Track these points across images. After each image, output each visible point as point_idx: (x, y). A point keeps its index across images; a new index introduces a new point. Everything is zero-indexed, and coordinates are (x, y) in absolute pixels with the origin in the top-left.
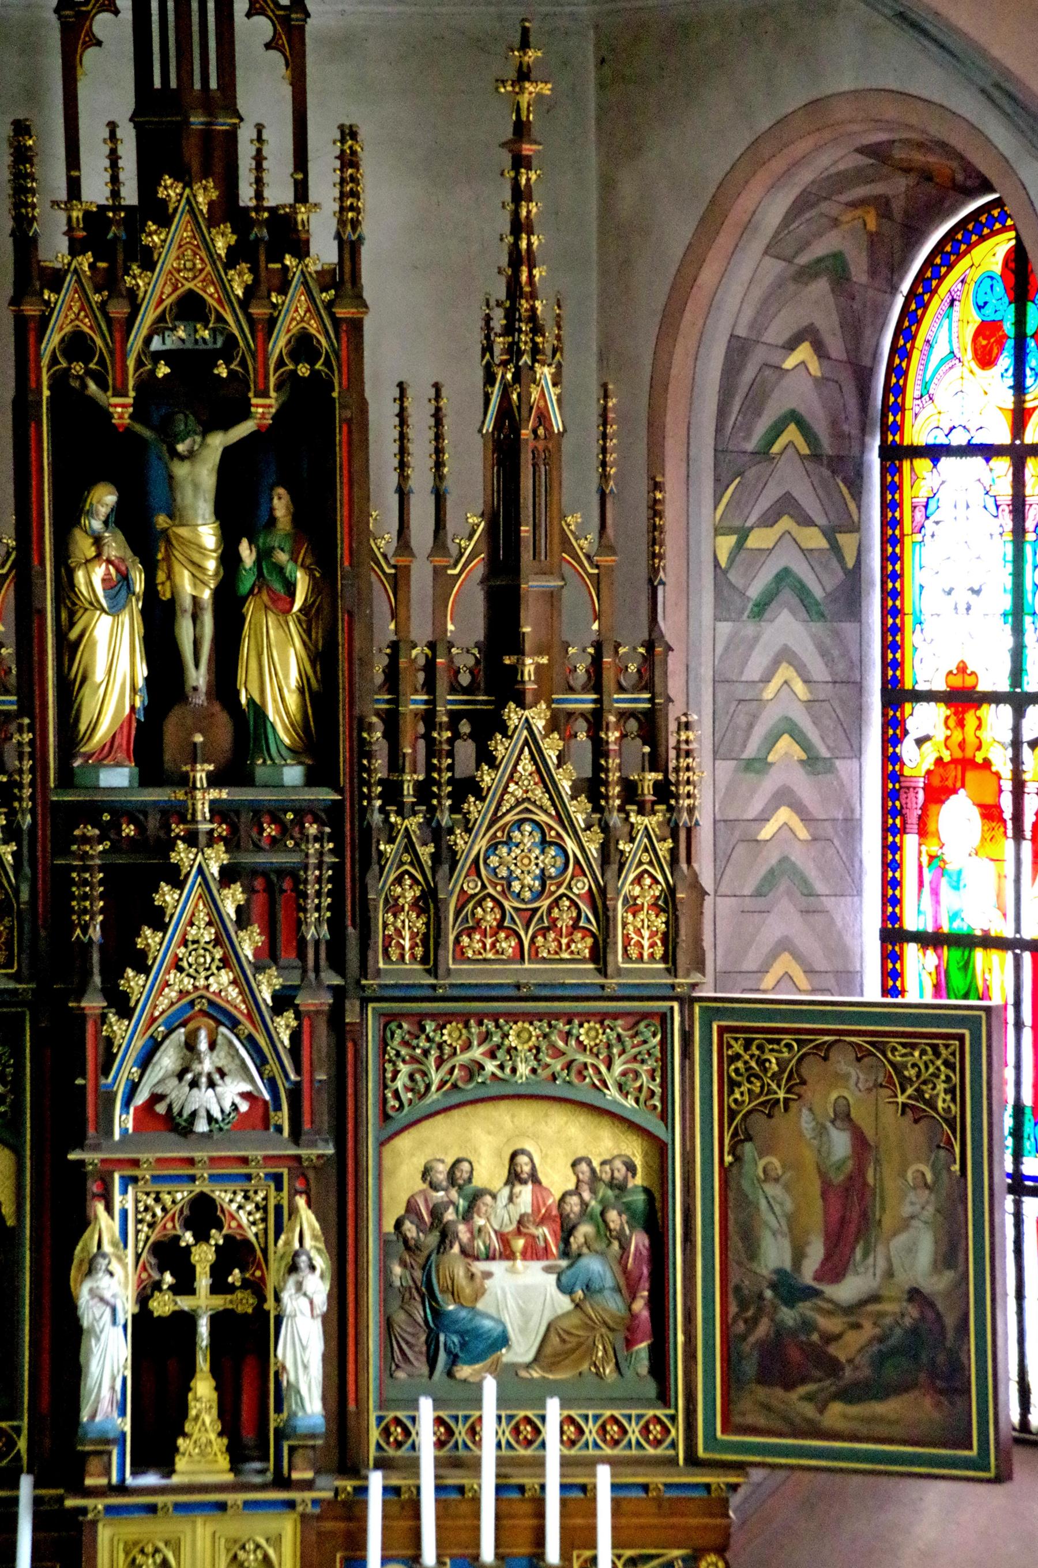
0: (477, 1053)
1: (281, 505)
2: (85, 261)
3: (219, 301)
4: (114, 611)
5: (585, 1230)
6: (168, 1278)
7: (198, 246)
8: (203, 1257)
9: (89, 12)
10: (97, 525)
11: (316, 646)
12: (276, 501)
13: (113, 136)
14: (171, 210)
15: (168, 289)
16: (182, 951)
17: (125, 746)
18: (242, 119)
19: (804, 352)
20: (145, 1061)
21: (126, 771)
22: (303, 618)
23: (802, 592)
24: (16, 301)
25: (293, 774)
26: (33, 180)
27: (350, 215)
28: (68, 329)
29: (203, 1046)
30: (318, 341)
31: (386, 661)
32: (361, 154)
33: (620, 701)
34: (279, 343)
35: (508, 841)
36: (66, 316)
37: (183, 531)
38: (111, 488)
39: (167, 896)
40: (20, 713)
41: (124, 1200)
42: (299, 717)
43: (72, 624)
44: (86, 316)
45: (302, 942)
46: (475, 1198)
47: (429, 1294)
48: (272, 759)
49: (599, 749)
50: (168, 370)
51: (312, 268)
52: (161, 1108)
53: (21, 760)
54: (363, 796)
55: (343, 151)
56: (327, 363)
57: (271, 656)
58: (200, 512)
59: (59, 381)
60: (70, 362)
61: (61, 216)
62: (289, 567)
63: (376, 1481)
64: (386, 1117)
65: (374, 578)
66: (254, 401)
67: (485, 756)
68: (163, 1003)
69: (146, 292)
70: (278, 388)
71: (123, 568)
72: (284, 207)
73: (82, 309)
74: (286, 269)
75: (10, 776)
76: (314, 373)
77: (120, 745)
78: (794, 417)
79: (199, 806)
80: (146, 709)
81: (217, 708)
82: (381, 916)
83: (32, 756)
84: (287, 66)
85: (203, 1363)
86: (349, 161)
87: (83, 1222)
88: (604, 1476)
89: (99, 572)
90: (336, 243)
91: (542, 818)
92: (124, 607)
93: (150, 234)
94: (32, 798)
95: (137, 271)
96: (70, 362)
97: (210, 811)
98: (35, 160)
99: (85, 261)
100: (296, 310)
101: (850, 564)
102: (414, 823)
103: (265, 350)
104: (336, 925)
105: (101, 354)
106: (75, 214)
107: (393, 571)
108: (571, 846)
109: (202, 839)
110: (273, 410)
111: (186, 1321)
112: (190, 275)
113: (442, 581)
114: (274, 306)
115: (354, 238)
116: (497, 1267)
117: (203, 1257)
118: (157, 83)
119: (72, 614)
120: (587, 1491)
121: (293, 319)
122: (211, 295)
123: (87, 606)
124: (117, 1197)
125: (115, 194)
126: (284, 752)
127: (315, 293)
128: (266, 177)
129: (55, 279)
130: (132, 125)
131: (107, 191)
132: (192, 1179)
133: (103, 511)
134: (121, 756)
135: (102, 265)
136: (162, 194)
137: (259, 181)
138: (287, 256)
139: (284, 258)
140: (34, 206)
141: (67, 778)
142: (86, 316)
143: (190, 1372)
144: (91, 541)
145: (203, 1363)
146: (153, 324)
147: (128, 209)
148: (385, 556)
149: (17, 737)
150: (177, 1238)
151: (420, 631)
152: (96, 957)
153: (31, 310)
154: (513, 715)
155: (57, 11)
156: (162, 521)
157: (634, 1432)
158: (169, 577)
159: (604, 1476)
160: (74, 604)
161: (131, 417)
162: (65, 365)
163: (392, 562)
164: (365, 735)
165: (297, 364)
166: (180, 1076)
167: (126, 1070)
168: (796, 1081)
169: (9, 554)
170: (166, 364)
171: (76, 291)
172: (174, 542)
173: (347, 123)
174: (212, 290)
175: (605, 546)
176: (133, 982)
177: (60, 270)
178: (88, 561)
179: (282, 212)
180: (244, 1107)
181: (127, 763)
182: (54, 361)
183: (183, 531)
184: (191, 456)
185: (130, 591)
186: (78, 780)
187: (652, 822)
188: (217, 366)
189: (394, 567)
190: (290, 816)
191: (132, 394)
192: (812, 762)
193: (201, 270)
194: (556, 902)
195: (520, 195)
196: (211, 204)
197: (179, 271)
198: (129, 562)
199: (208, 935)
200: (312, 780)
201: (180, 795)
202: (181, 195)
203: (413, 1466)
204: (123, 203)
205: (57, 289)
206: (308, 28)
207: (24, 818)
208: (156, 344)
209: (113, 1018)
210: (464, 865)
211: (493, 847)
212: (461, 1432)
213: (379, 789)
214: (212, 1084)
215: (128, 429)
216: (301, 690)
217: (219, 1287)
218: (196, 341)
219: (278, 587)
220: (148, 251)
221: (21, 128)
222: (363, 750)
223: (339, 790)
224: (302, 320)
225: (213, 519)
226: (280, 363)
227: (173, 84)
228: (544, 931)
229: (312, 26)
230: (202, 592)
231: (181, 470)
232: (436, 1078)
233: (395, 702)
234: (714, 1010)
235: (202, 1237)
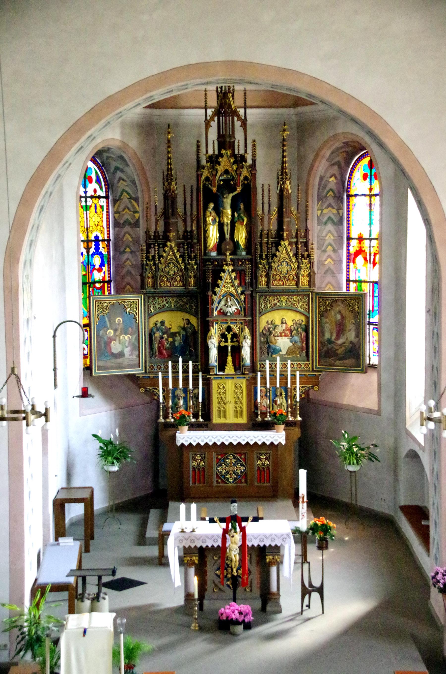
0: (276, 301)
1: (242, 206)
2: (209, 164)
4: (213, 225)
5: (294, 332)
6: (223, 340)
8: (229, 336)
10: (210, 210)
13: (214, 143)
16: (225, 284)
19: (333, 178)
20: (219, 303)
23: (333, 221)
24: (197, 171)
25: (244, 253)
29: (229, 300)
33: (301, 240)
34: (242, 178)
35: (281, 265)
37: (225, 211)
39: (222, 274)
40: (197, 243)
41: (216, 326)
45: (246, 282)
46: (275, 326)
47: (267, 343)
49: (297, 248)
52: (222, 311)
56: (250, 181)
59: (204, 185)
61: (205, 156)
63: (259, 374)
64: (260, 313)
67: (277, 250)
68: (222, 293)
70: (242, 185)
74: (243, 165)
76: (248, 183)
78: (331, 190)
82: (259, 278)
85: (229, 354)
86: (254, 146)
87: (209, 330)
88: (298, 373)
89: (211, 218)
91: (287, 260)
99: (209, 164)
101: (341, 215)
102: (265, 262)
104: (251, 279)
108: (292, 265)
109: (228, 265)
111: (226, 347)
113: (270, 219)
116: (279, 338)
117: (229, 336)
118: (221, 133)
119: (206, 226)
120: (295, 376)
124: (215, 326)
125: (214, 152)
129: (203, 167)
131: (212, 152)
132: (227, 323)
133: (211, 207)
136: (222, 152)
137: (239, 150)
141: (205, 254)
143: (227, 355)
145: (229, 354)
147: (216, 155)
150: (225, 333)
151: (266, 228)
152: (210, 285)
153: (199, 173)
154: (282, 243)
155: (205, 121)
156: (221, 209)
157: (303, 366)
158: (223, 219)
159: (298, 373)
166: (225, 305)
167: (216, 304)
168: (331, 306)
175: (298, 213)
176: (217, 289)
180: (236, 311)
182: (203, 182)
184: (226, 198)
185: (216, 221)
187: (306, 261)
192: (334, 251)
194: (289, 275)
195: (284, 151)
199: (229, 281)
200: (247, 254)
203: (265, 371)
205: (204, 169)
208: (221, 178)
209: (213, 295)
210: (274, 269)
211: (279, 266)
212: (273, 365)
214: (230, 307)
215: (216, 193)
217: (232, 341)
219: (241, 220)
221: (198, 142)
222: (256, 249)
226: (242, 181)
227: (224, 133)
228: (288, 280)
231: (225, 200)
232: (269, 306)
233: (261, 240)
234: (317, 294)
235: (229, 333)
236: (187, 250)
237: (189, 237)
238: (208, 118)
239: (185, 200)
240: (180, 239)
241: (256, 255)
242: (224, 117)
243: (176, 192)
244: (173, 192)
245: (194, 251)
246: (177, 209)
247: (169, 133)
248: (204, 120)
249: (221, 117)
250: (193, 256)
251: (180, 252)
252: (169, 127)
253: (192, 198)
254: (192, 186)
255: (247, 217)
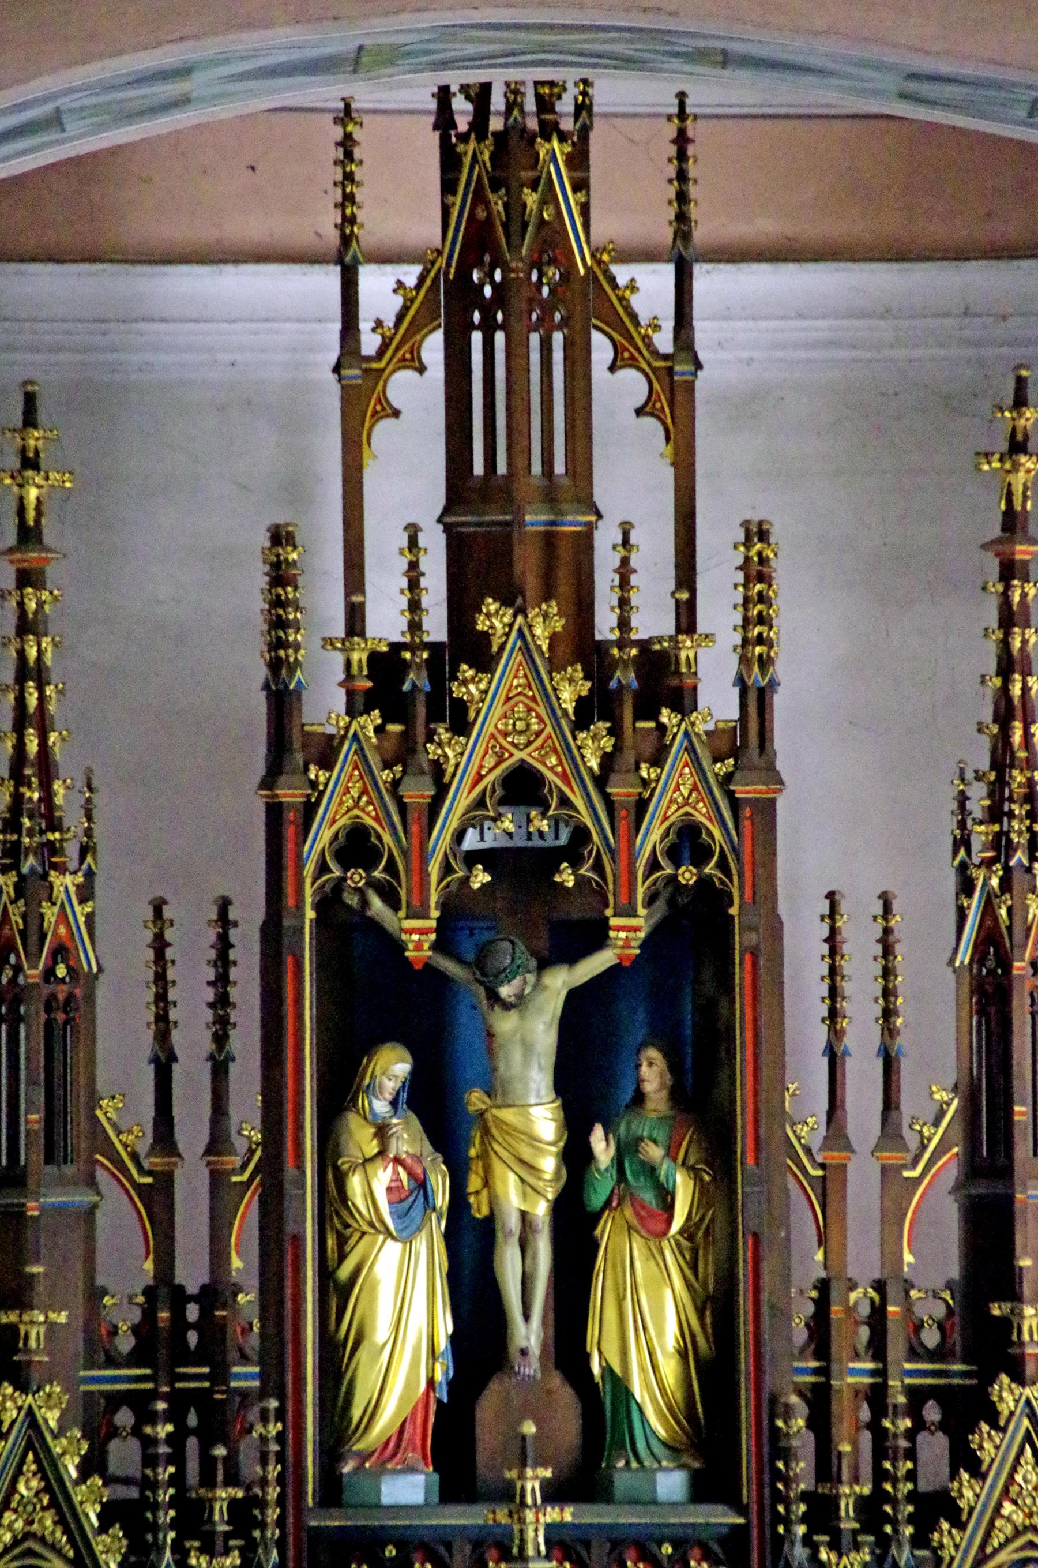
3: (564, 776)
4: (406, 1236)
7: (533, 699)
9: (383, 370)
10: (381, 1107)
11: (704, 1286)
12: (644, 1069)
13: (413, 544)
14: (495, 648)
15: (490, 761)
17: (418, 1443)
18: (600, 516)
21: (420, 1478)
22: (685, 1243)
24: (269, 782)
26: (297, 608)
27: (758, 650)
28: (342, 822)
30: (711, 835)
31: (810, 1309)
32: (773, 564)
36: (341, 803)
37: (507, 1115)
38: (402, 1052)
40: (263, 1394)
42: (679, 1396)
43: (342, 1257)
44: (370, 802)
48: (639, 1460)
50: (488, 878)
51: (701, 728)
53: (264, 1463)
54: (777, 1519)
55: (747, 559)
56: (723, 865)
57: (637, 1302)
58: (533, 1086)
60: (346, 869)
61: (339, 658)
62: (665, 1168)
65: (792, 1184)
66: (614, 922)
69: (457, 765)
70: (650, 900)
71: (419, 1171)
72: (660, 640)
73: (364, 792)
74: (662, 728)
75: (248, 1488)
76: (704, 882)
77: (412, 1441)
79: (531, 1534)
80: (451, 1384)
81: (556, 1380)
83: (280, 1458)
84: (668, 439)
89: (382, 1177)
90: (736, 691)
92: (419, 1229)
93: (465, 683)
94: (280, 1522)
95: (445, 736)
96: (346, 869)
97: (547, 1542)
98: (301, 581)
100: (677, 788)
103: (631, 843)
105: (391, 856)
106: (355, 656)
107: (820, 1173)
110: (642, 935)
112: (522, 740)
114: (645, 783)
115: (763, 683)
118: (479, 469)
119: (342, 1241)
121: (672, 801)
122: (552, 769)
123: (365, 1228)
125: (415, 626)
126: (658, 1449)
127: (706, 763)
128: (635, 598)
130: (441, 527)
131: (403, 623)
133: (390, 1086)
134: (413, 1456)
135: (394, 728)
136: (482, 624)
137: (624, 603)
138: (665, 711)
139: (659, 713)
140: (297, 647)
142: (370, 802)
144: (372, 1130)
146: (467, 812)
147: (434, 647)
148: (808, 1151)
149: (259, 1429)
153: (290, 794)
155: (337, 369)
156: (476, 1100)
158: (486, 1183)
160: (347, 1226)
161: (435, 947)
162: (337, 873)
163: (820, 1159)
164: (780, 1423)
165: (678, 866)
169: (251, 1152)
170: (485, 870)
171: (356, 767)
172: (494, 1131)
173: (756, 517)
174: (554, 760)
177: (331, 737)
178: (366, 1161)
179: (657, 647)
181: (421, 1466)
182: (323, 868)
183: (507, 1115)
184: (519, 1003)
185: (428, 1204)
186: (347, 1496)
188: (560, 872)
189: (823, 1166)
190: (667, 1549)
191: (435, 914)
193: (538, 734)
196: (554, 639)
197: (506, 735)
198: (427, 1162)
201: (502, 1517)
202: (511, 626)
204: (426, 638)
205: (327, 763)
206: (698, 384)
207: (267, 1552)
208: (471, 841)
213: (803, 1508)
215: (428, 967)
216: (683, 1354)
218: (529, 835)
219: (648, 1197)
220: (460, 707)
221: (280, 537)
223: (742, 1510)
224: (686, 803)
225: (553, 1096)
226: (654, 865)
227: (502, 468)
229: (703, 382)
230: (535, 1205)
231: (505, 1024)
233: (824, 1371)
236: (178, 1458)
237: (193, 1338)
238: (369, 343)
239: (163, 1025)
240: (111, 1362)
241: (778, 1497)
242: (500, 337)
243: (88, 959)
244: (60, 952)
245: (231, 1461)
246: (94, 1100)
247: (30, 462)
248: (333, 356)
249: (477, 337)
250: (220, 1512)
251: (109, 1481)
252: (30, 420)
253: (222, 1002)
254: (224, 905)
255: (693, 1171)
